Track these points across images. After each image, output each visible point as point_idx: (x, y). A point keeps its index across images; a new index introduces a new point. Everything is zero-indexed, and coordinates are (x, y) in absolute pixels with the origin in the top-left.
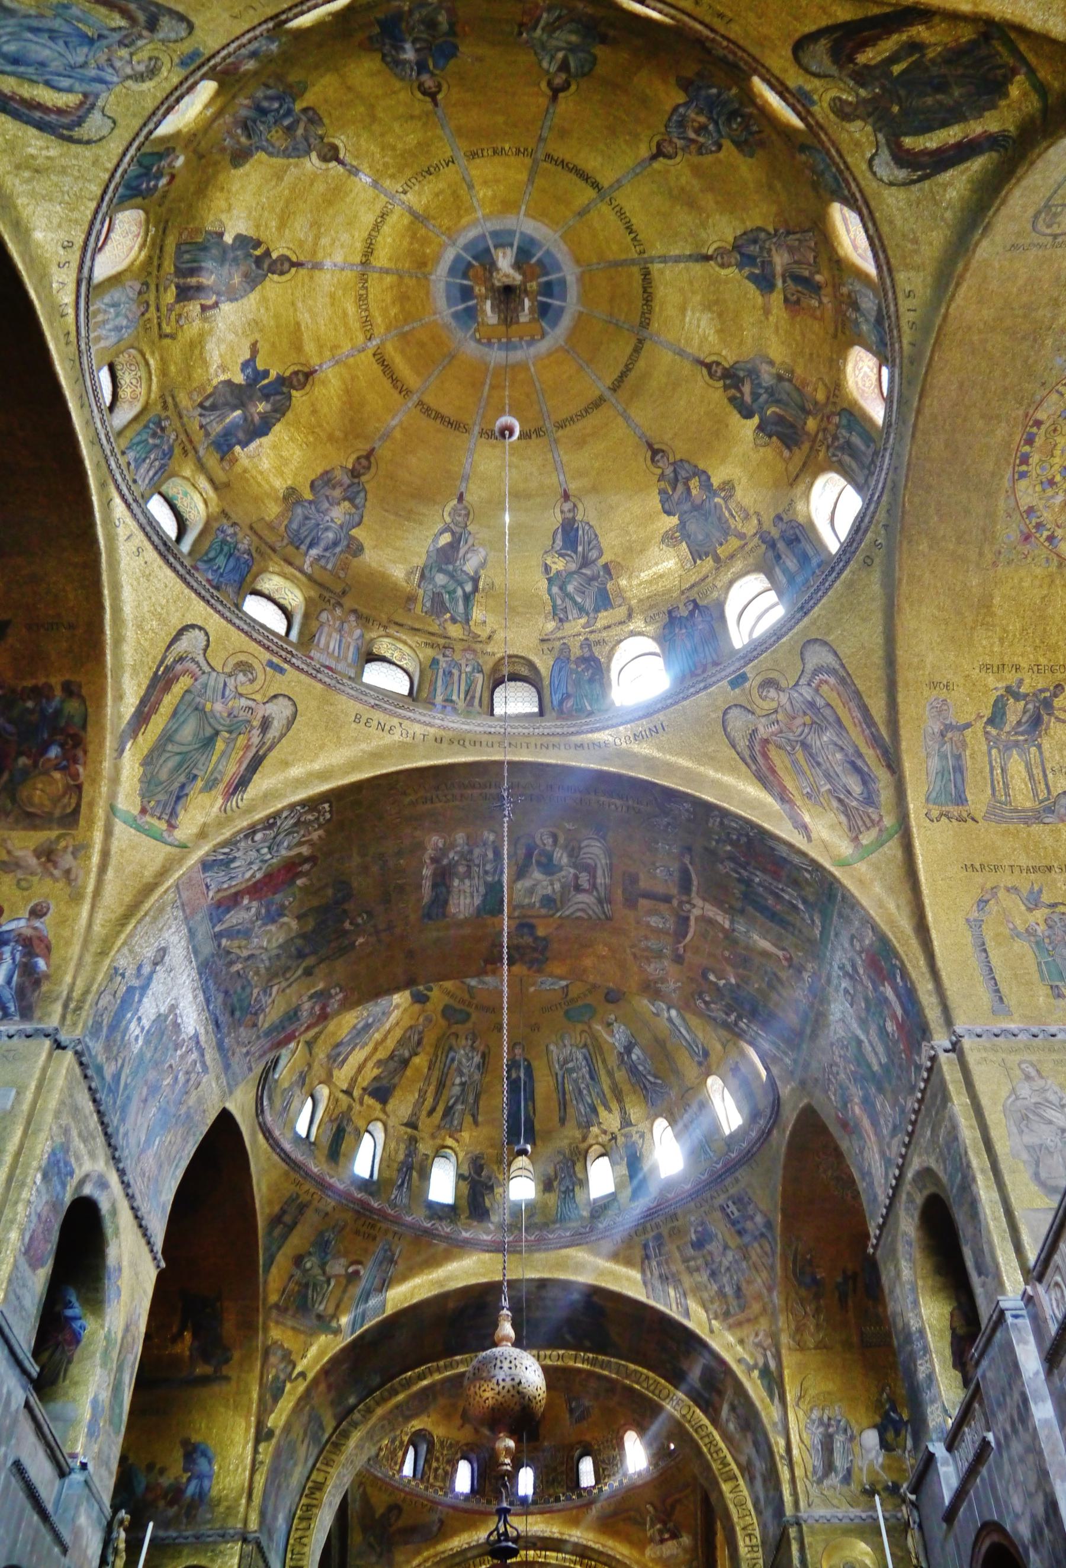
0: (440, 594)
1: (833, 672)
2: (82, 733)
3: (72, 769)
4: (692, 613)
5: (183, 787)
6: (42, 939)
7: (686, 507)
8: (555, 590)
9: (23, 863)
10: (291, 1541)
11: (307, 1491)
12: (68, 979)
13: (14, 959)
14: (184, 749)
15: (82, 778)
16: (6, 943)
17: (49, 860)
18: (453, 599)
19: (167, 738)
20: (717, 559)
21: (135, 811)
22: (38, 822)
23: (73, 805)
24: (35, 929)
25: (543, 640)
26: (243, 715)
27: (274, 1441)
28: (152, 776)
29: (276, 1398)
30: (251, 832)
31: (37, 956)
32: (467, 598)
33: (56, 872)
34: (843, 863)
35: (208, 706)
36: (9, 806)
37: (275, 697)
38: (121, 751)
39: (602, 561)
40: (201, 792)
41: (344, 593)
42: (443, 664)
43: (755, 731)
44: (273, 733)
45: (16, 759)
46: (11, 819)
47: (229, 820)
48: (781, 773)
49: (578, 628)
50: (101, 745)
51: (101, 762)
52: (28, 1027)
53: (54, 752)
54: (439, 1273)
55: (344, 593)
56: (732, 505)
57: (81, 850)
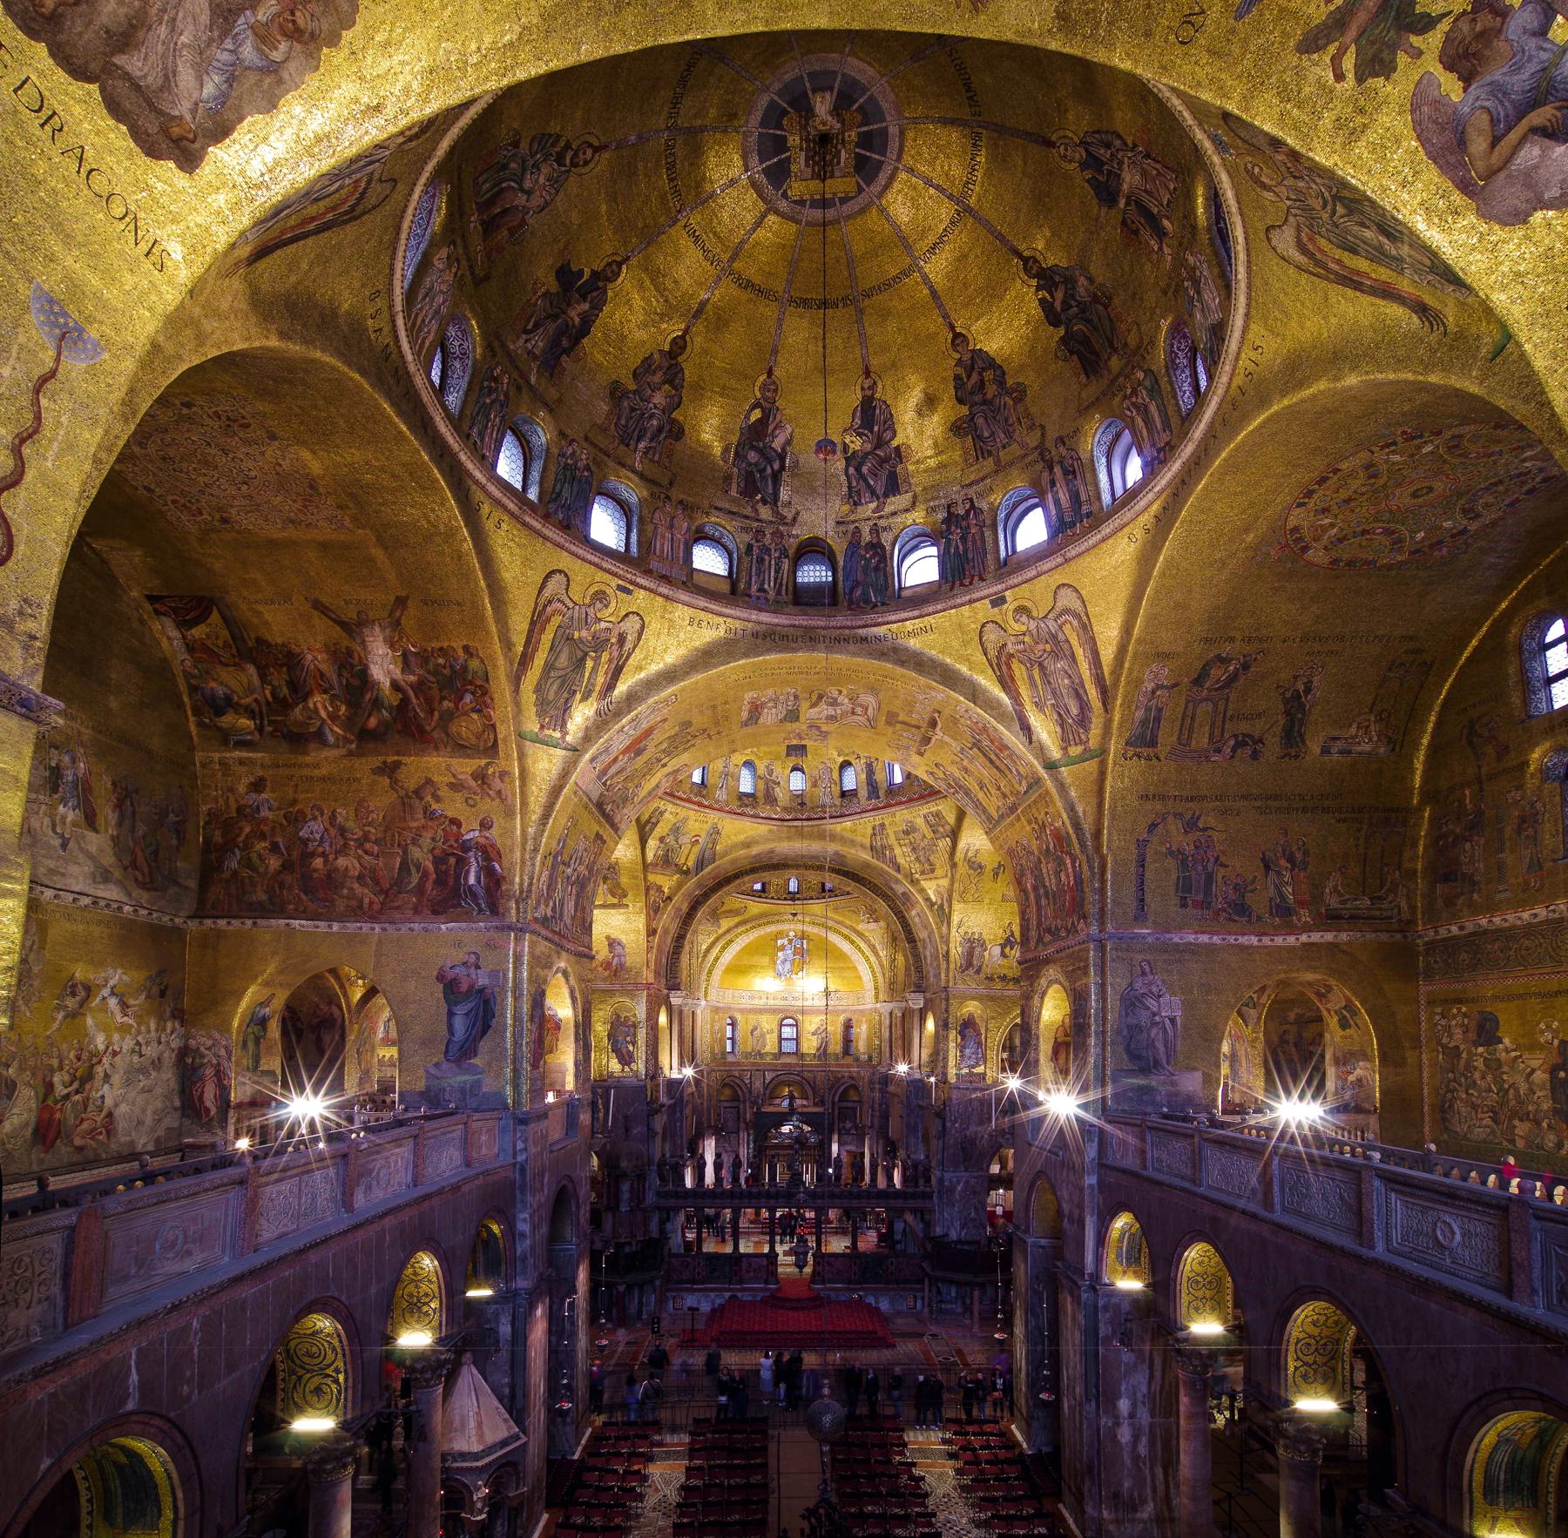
0: (751, 473)
1: (1077, 616)
4: (968, 512)
6: (493, 846)
7: (978, 398)
8: (851, 470)
14: (561, 673)
16: (469, 849)
18: (763, 478)
19: (549, 667)
20: (998, 462)
25: (838, 523)
26: (603, 636)
32: (776, 478)
35: (576, 635)
37: (627, 615)
39: (895, 443)
41: (671, 484)
42: (756, 551)
43: (1005, 645)
44: (628, 645)
49: (869, 513)
55: (671, 484)
56: (1020, 408)
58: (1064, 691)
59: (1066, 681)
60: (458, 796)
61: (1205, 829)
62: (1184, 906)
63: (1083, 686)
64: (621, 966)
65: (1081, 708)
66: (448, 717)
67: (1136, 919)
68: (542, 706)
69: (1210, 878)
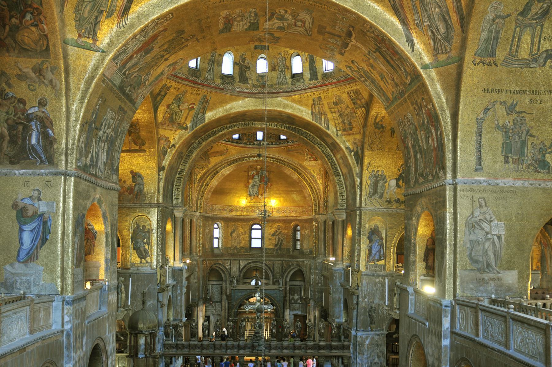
2: (41, 8)
3: (40, 26)
5: (97, 18)
6: (48, 118)
9: (29, 76)
10: (174, 190)
11: (178, 173)
12: (64, 141)
13: (37, 129)
15: (47, 32)
16: (32, 120)
17: (40, 75)
21: (76, 38)
22: (30, 53)
23: (45, 46)
24: (43, 112)
27: (165, 171)
28: (80, 17)
29: (165, 153)
30: (135, 36)
31: (48, 128)
33: (45, 81)
34: (425, 67)
36: (14, 45)
38: (62, 11)
40: (106, 19)
45: (10, 19)
46: (16, 51)
47: (124, 33)
48: (406, 10)
50: (52, 14)
51: (54, 23)
52: (53, 170)
53: (28, 17)
54: (228, 106)
57: (54, 69)
58: (436, 17)
59: (437, 10)
60: (24, 85)
61: (520, 112)
62: (507, 162)
63: (448, 14)
64: (141, 191)
65: (447, 29)
66: (16, 29)
67: (476, 170)
68: (80, 21)
69: (523, 144)
